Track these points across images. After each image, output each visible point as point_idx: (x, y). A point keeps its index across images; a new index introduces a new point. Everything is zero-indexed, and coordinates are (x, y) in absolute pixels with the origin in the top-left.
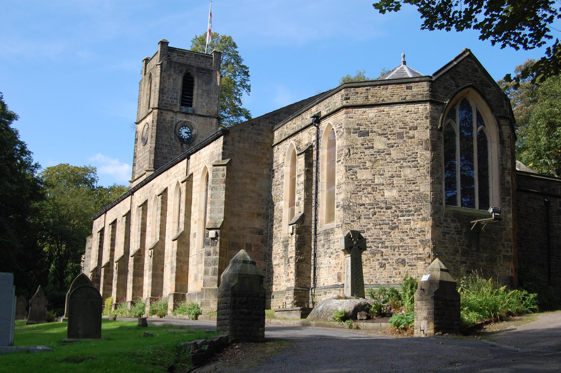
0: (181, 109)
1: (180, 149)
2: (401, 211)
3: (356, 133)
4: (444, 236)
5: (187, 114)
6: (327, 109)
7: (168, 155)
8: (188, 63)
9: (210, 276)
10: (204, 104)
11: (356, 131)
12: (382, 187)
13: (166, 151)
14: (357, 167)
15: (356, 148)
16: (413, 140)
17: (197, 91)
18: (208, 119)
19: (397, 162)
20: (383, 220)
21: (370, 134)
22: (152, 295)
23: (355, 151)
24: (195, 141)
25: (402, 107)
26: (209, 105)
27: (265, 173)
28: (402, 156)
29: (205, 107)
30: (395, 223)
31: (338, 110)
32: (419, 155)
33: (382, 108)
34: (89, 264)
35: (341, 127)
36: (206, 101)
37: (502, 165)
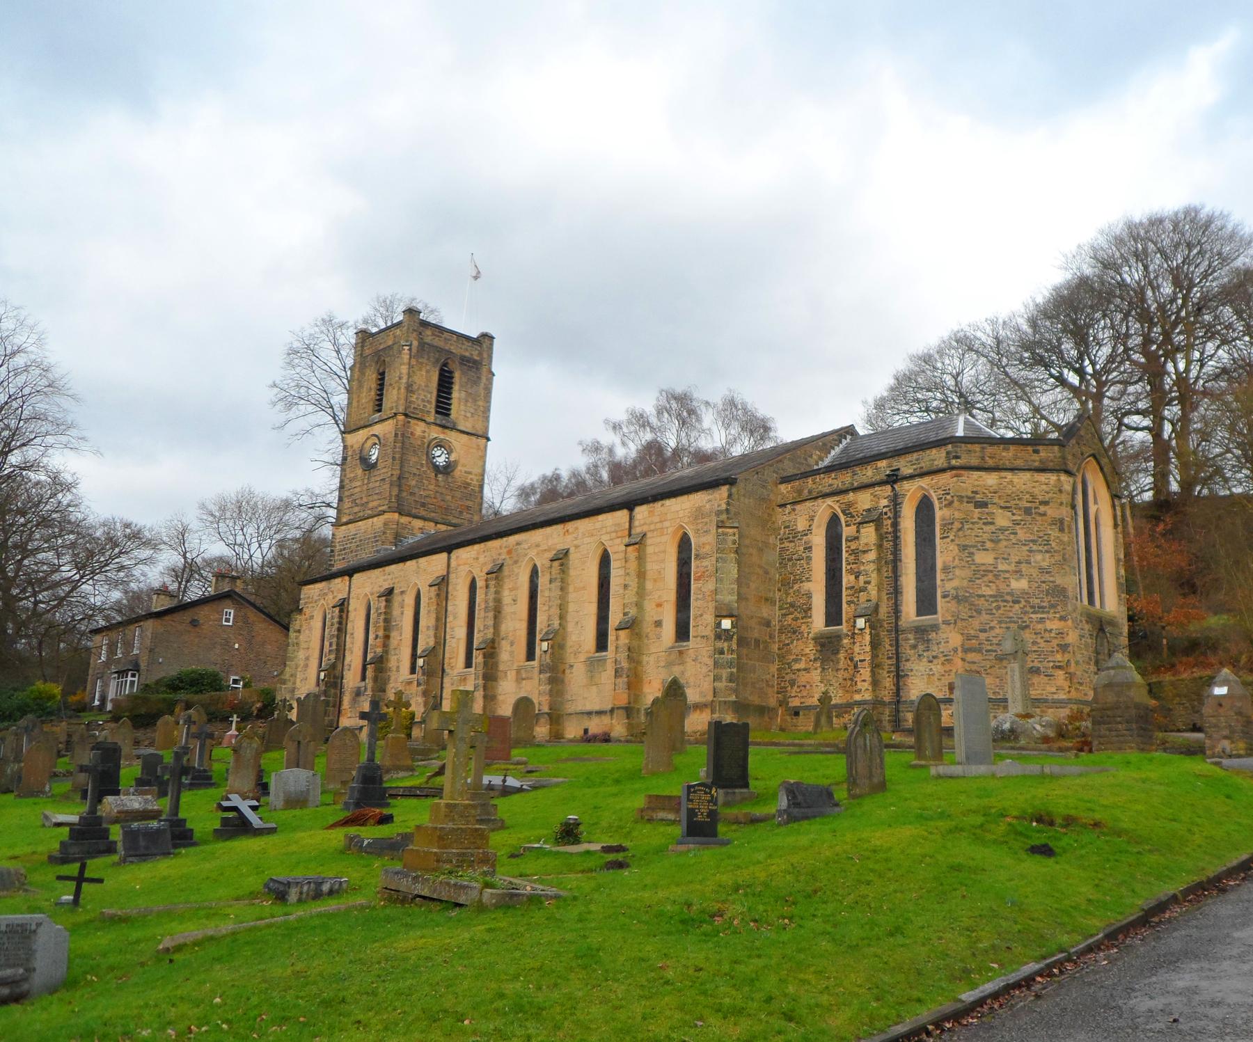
1: (433, 481)
2: (1032, 607)
5: (444, 427)
11: (970, 500)
12: (1007, 575)
13: (414, 483)
14: (971, 546)
16: (1044, 518)
18: (474, 438)
23: (971, 526)
25: (1028, 475)
28: (1032, 538)
31: (943, 470)
33: (1004, 474)
35: (948, 494)
36: (472, 411)
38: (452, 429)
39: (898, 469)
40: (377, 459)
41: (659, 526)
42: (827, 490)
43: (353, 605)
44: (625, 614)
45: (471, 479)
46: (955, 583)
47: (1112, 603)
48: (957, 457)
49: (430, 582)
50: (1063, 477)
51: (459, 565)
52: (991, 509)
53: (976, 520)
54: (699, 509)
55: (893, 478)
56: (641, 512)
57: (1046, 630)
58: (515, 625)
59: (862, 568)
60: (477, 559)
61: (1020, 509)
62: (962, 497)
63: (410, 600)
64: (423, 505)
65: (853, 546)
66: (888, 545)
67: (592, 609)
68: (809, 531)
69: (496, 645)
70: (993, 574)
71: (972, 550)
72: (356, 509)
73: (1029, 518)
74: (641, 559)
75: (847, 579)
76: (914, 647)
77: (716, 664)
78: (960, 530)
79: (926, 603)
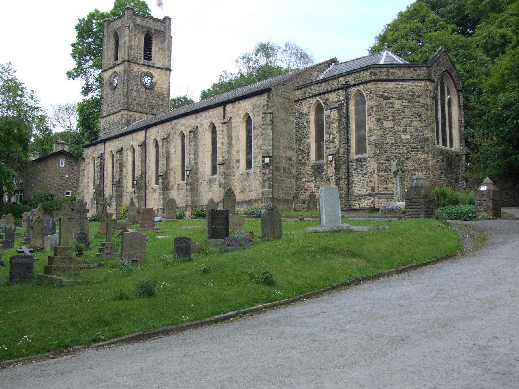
0: (144, 62)
1: (144, 93)
3: (382, 97)
4: (436, 164)
5: (148, 66)
6: (356, 80)
7: (136, 98)
8: (148, 26)
9: (266, 190)
10: (161, 59)
11: (381, 96)
12: (400, 133)
14: (383, 119)
15: (382, 107)
17: (155, 48)
18: (164, 71)
19: (409, 118)
20: (401, 154)
21: (391, 99)
22: (192, 203)
23: (382, 109)
24: (155, 88)
25: (410, 83)
26: (164, 60)
27: (291, 119)
28: (412, 114)
29: (161, 61)
30: (409, 156)
32: (422, 114)
33: (398, 82)
34: (84, 182)
35: (371, 93)
36: (162, 56)
37: (460, 120)
38: (152, 67)
39: (348, 81)
40: (117, 84)
41: (237, 113)
42: (317, 93)
43: (107, 157)
44: (223, 157)
45: (163, 91)
46: (374, 137)
47: (457, 146)
48: (375, 75)
49: (137, 145)
50: (428, 83)
51: (150, 135)
52: (392, 100)
53: (384, 106)
54: (255, 104)
55: (347, 86)
56: (229, 107)
57: (418, 159)
58: (176, 163)
59: (332, 131)
60: (158, 132)
61: (407, 100)
62: (378, 95)
63: (130, 154)
64: (140, 105)
65: (328, 120)
66: (344, 119)
67: (209, 155)
68: (308, 114)
69: (168, 174)
70: (395, 133)
71: (382, 121)
72: (109, 109)
73: (411, 104)
74: (229, 130)
75: (326, 137)
76: (356, 169)
77: (263, 180)
78: (376, 111)
79: (361, 149)
